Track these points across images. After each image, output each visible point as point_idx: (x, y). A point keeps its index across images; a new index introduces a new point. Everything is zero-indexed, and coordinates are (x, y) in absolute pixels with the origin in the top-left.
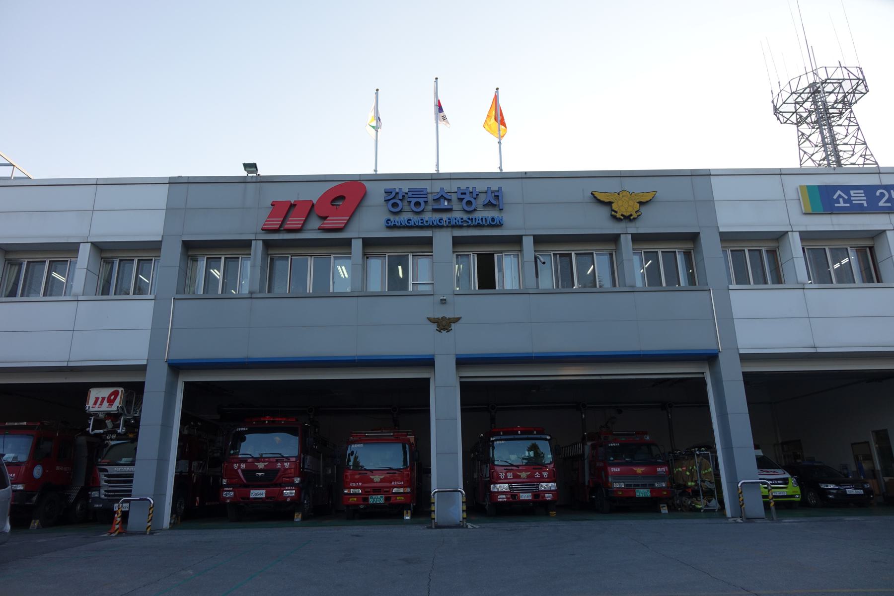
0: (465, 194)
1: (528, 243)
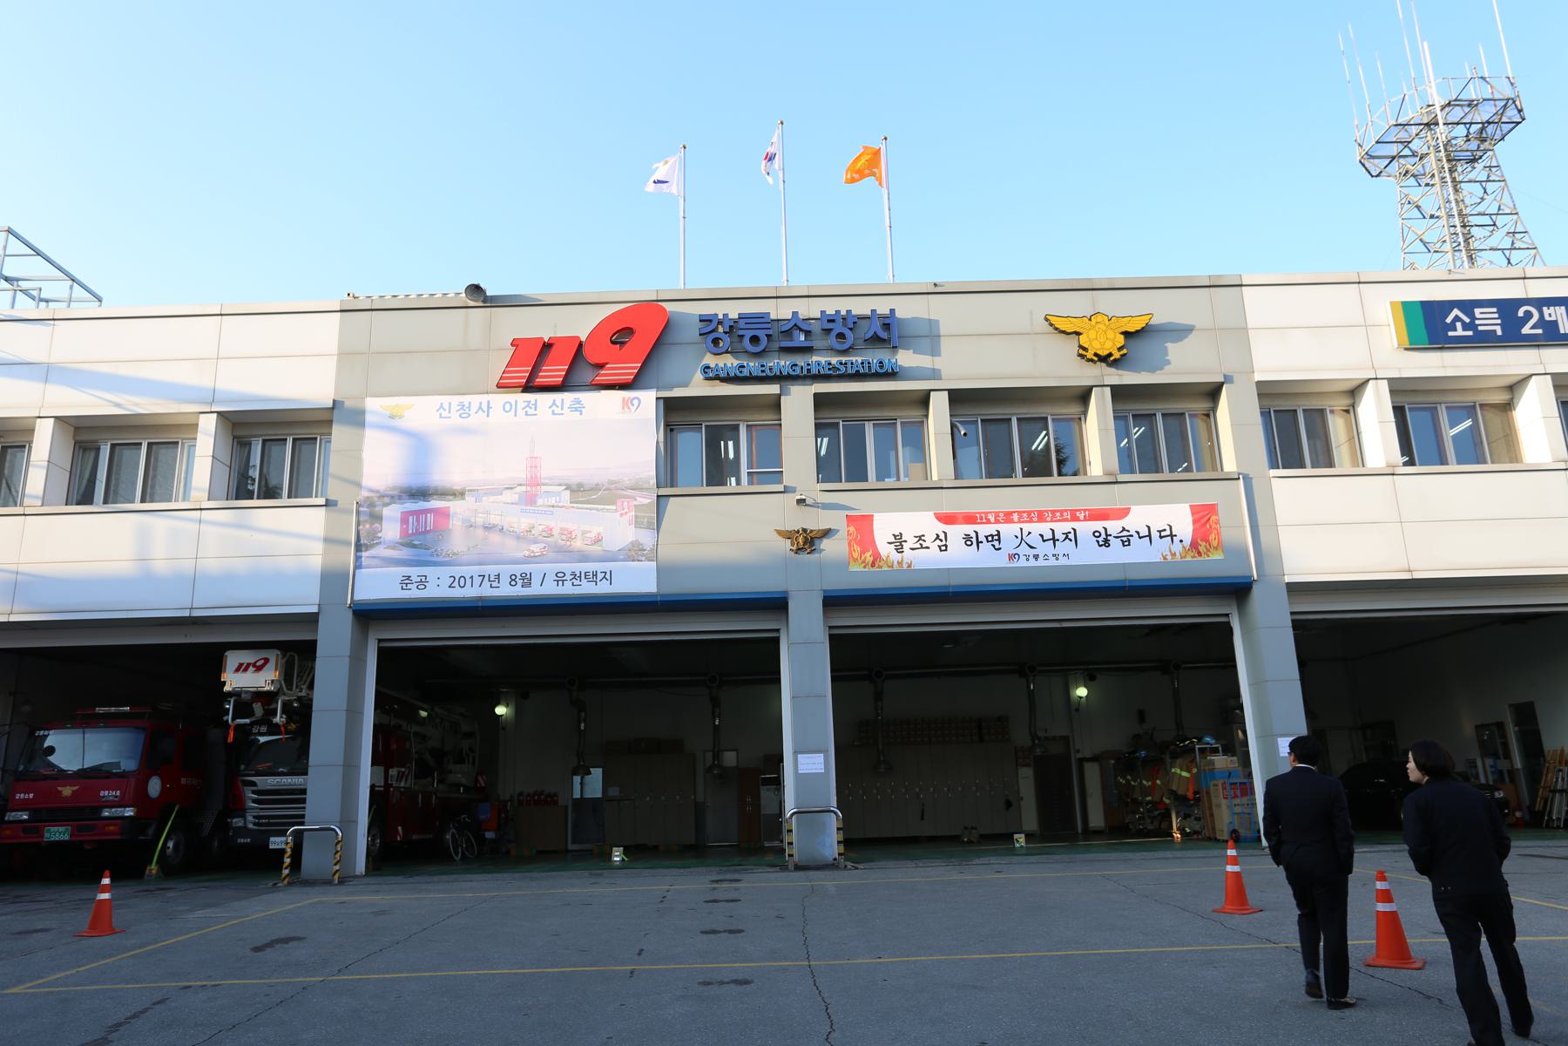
0: (833, 321)
1: (939, 406)
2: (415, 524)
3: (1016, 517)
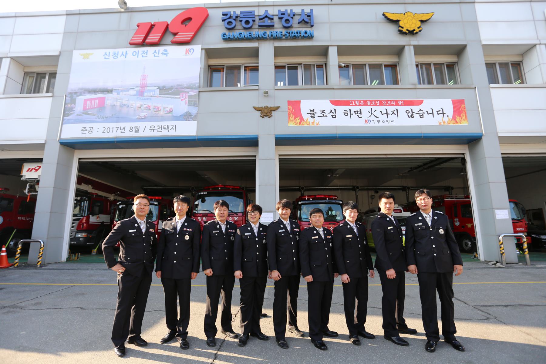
0: (284, 14)
2: (90, 104)
3: (369, 103)
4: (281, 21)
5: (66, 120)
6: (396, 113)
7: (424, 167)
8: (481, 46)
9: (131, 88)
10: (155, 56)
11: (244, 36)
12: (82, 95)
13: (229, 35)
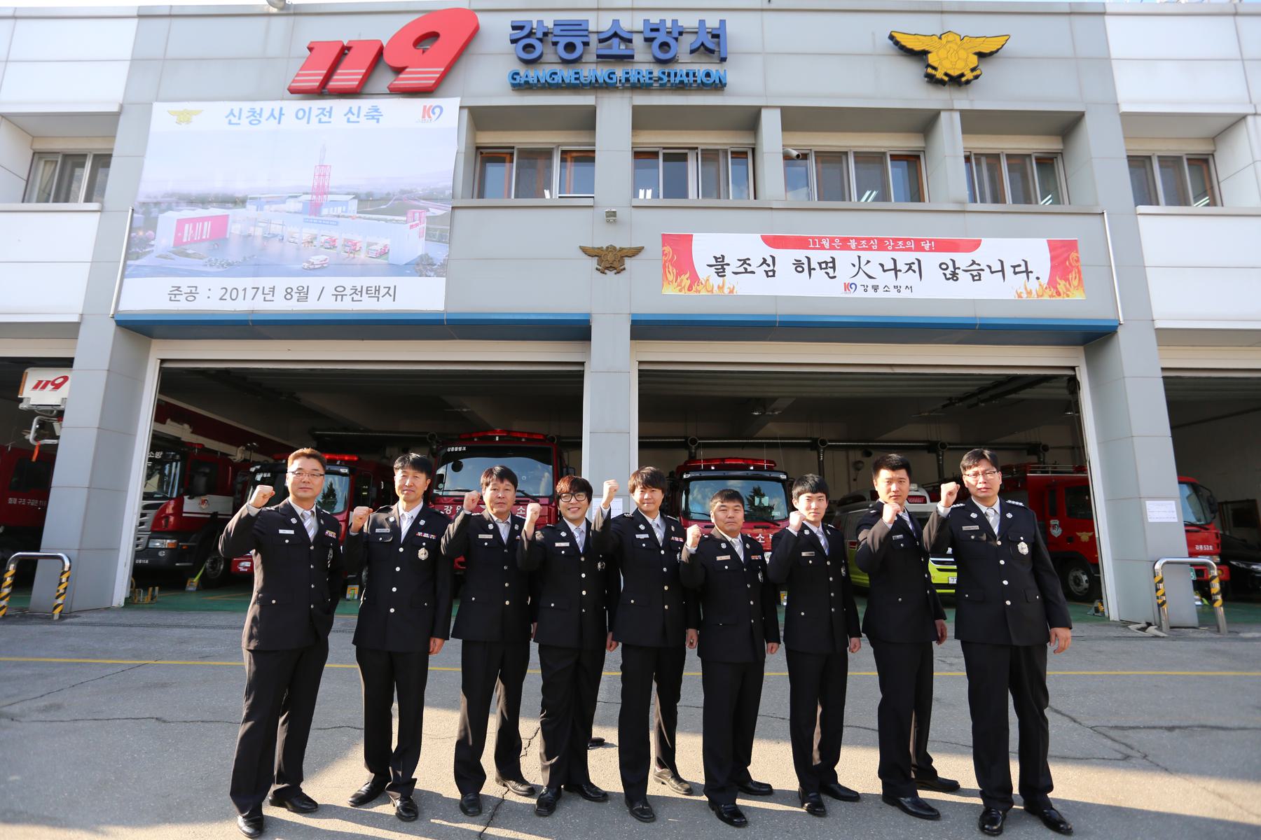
0: (657, 30)
2: (191, 232)
3: (853, 244)
4: (650, 47)
5: (132, 268)
6: (916, 268)
7: (980, 396)
8: (1118, 119)
9: (291, 195)
10: (348, 121)
11: (563, 80)
12: (171, 210)
13: (527, 76)
